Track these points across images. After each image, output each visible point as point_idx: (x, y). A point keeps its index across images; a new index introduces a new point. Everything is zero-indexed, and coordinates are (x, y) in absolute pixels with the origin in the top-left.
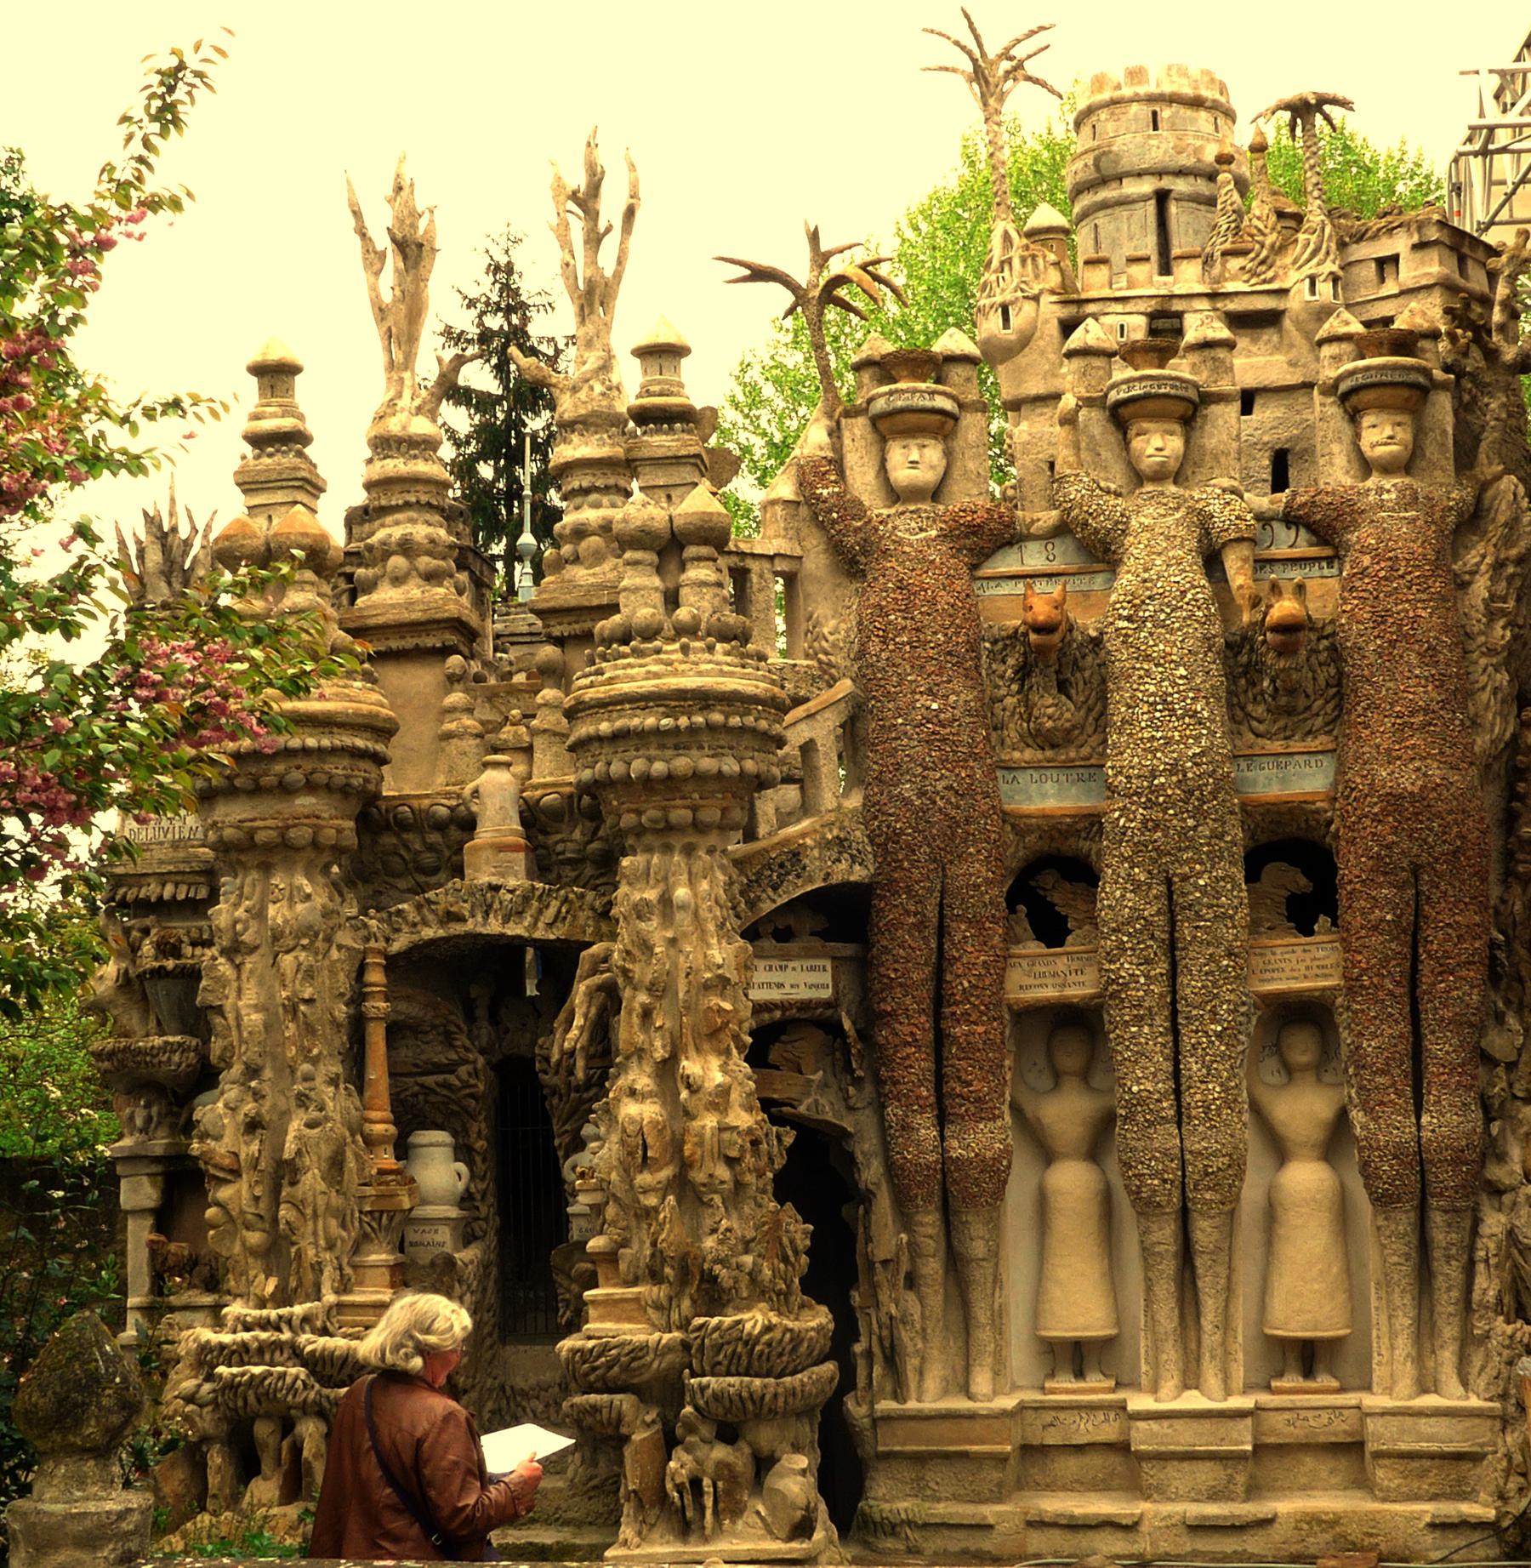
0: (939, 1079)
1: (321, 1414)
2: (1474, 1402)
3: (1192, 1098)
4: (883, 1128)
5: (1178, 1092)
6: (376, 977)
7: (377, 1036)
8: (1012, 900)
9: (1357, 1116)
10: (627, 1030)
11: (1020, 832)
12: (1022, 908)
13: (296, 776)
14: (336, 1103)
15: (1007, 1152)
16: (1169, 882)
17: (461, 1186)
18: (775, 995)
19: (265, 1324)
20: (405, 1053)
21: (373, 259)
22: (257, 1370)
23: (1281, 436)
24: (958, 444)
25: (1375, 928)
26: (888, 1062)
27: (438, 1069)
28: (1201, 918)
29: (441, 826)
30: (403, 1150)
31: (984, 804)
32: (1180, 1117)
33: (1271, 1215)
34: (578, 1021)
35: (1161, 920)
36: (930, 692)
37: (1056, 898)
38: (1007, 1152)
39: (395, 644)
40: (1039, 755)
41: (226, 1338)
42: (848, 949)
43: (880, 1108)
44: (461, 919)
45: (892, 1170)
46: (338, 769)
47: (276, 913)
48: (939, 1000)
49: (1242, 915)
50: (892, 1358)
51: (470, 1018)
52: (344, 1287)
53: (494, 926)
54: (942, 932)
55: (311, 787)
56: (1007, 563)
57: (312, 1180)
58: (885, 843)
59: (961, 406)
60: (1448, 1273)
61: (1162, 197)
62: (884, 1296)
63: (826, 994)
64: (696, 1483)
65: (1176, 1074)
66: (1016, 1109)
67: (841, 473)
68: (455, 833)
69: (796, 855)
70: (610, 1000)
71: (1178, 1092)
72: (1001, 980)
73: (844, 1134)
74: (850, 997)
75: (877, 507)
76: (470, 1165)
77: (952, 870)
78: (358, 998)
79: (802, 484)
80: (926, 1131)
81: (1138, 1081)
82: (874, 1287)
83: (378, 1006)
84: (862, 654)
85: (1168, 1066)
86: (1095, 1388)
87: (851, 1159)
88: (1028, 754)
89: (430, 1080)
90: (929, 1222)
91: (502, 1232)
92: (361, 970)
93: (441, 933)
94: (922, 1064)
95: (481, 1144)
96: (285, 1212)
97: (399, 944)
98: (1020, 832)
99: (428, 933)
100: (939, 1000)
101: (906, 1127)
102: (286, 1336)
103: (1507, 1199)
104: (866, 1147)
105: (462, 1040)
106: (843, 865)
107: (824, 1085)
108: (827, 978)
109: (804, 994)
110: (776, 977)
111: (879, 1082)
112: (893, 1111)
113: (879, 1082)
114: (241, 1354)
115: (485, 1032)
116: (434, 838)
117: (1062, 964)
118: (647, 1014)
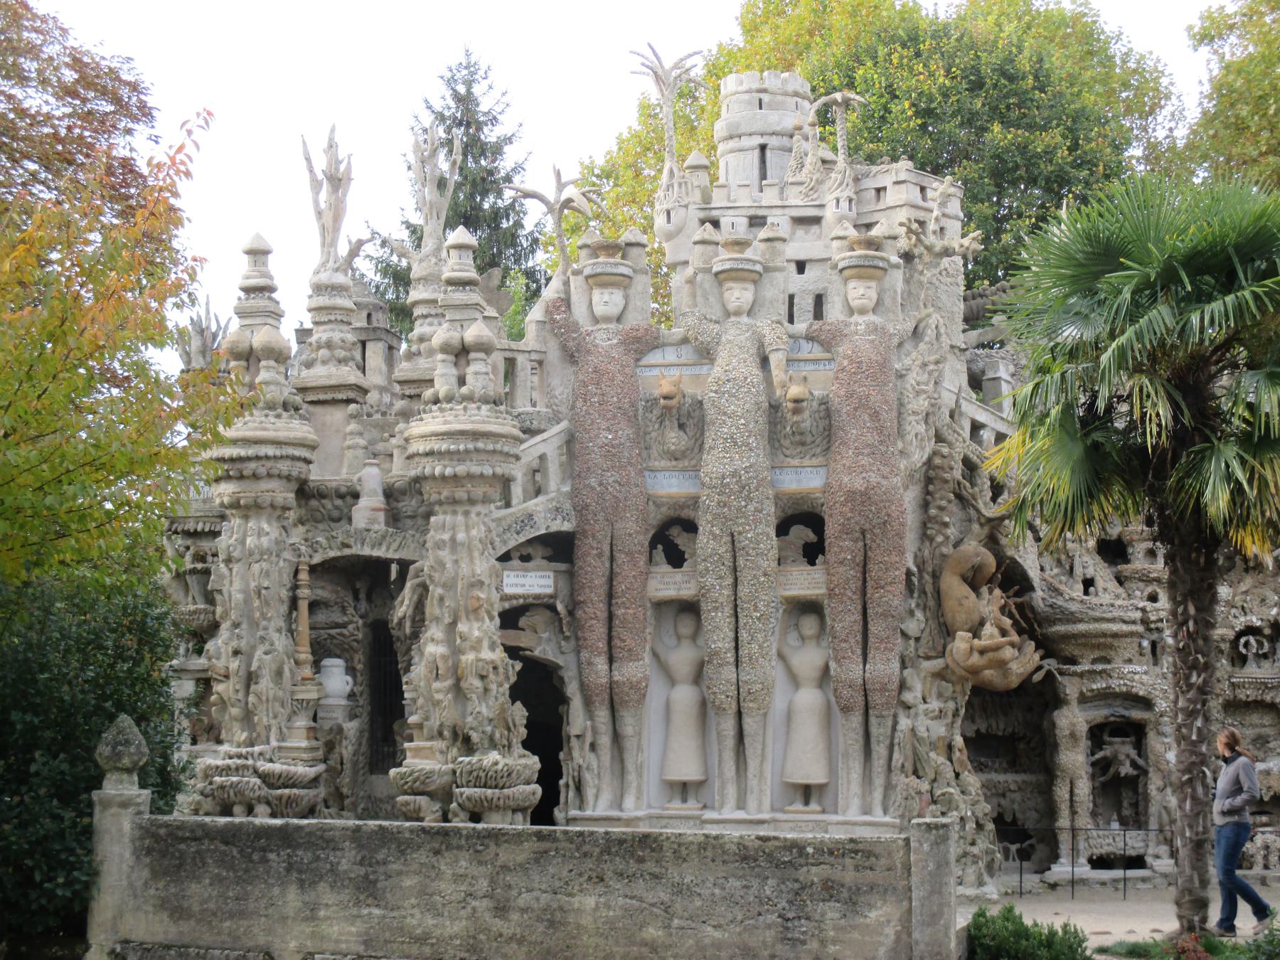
2: (887, 819)
4: (579, 664)
5: (737, 648)
6: (304, 576)
9: (833, 665)
10: (431, 609)
11: (658, 505)
12: (660, 547)
13: (262, 471)
14: (281, 642)
15: (646, 678)
16: (732, 535)
17: (348, 688)
18: (519, 591)
19: (240, 756)
20: (322, 617)
22: (235, 779)
23: (817, 287)
24: (632, 292)
25: (841, 563)
26: (581, 628)
27: (337, 626)
28: (748, 554)
29: (342, 497)
30: (317, 666)
31: (635, 491)
32: (737, 663)
33: (789, 716)
34: (406, 602)
35: (728, 555)
36: (608, 429)
37: (678, 541)
38: (646, 678)
39: (322, 397)
40: (669, 464)
41: (220, 762)
42: (563, 566)
43: (578, 652)
44: (348, 546)
45: (583, 687)
46: (284, 467)
48: (610, 596)
49: (774, 553)
50: (579, 788)
51: (356, 598)
52: (282, 738)
53: (367, 551)
54: (612, 558)
55: (269, 476)
56: (654, 358)
57: (265, 684)
58: (581, 510)
59: (635, 271)
60: (880, 750)
62: (576, 754)
63: (550, 591)
65: (736, 639)
66: (655, 655)
67: (569, 306)
68: (349, 499)
69: (530, 516)
71: (737, 648)
72: (645, 585)
73: (558, 667)
74: (564, 592)
75: (586, 326)
76: (354, 677)
77: (617, 526)
78: (295, 587)
79: (547, 312)
80: (601, 664)
81: (714, 642)
82: (570, 749)
83: (304, 592)
84: (573, 407)
85: (732, 635)
86: (691, 807)
87: (561, 679)
88: (663, 463)
89: (333, 632)
90: (603, 715)
91: (372, 715)
92: (296, 572)
93: (339, 554)
94: (600, 630)
95: (360, 667)
96: (251, 699)
97: (317, 559)
98: (658, 505)
99: (332, 554)
100: (610, 596)
101: (590, 664)
102: (250, 762)
103: (912, 711)
105: (351, 611)
106: (558, 521)
107: (549, 640)
108: (551, 582)
109: (537, 590)
110: (521, 581)
112: (585, 655)
113: (577, 639)
114: (226, 770)
115: (363, 606)
116: (339, 502)
118: (441, 599)
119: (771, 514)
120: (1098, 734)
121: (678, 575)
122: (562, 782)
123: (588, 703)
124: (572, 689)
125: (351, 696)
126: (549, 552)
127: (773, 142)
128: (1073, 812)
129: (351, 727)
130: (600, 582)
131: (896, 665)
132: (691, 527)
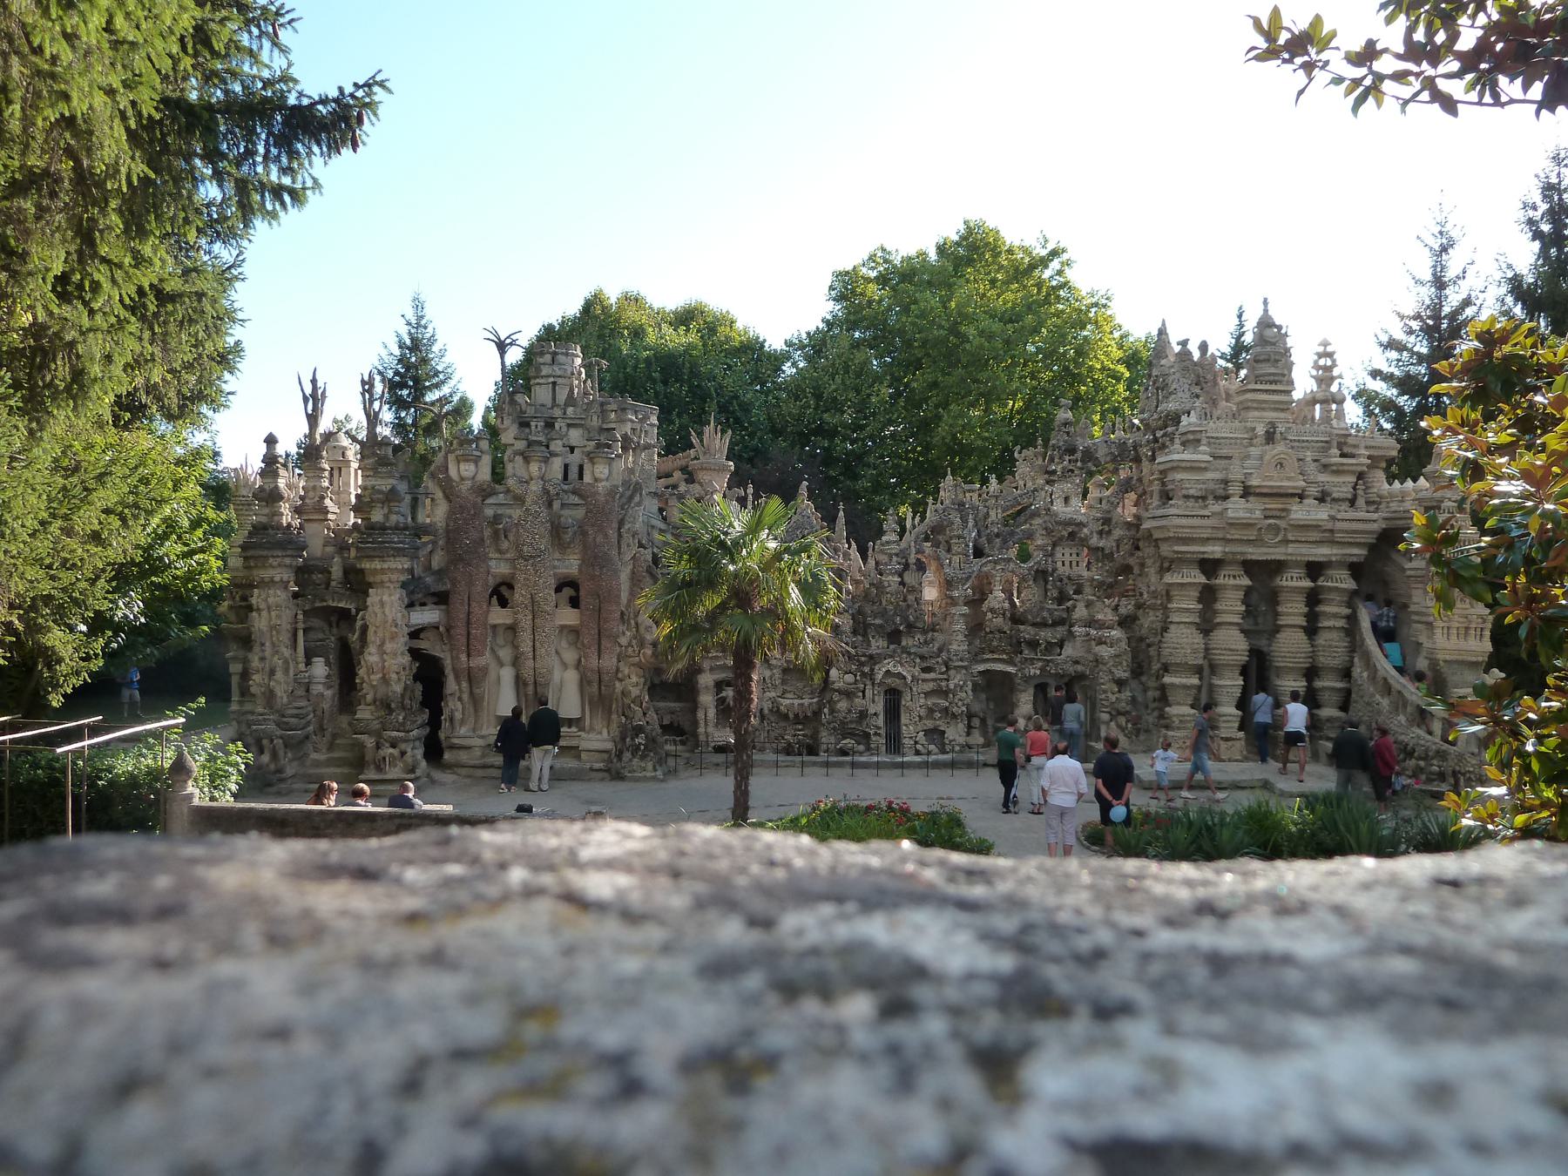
0: (468, 645)
1: (281, 737)
3: (538, 653)
7: (300, 633)
8: (491, 596)
11: (494, 577)
18: (420, 621)
20: (312, 635)
21: (306, 400)
32: (534, 658)
42: (443, 607)
45: (454, 669)
47: (270, 600)
48: (468, 623)
51: (331, 626)
61: (554, 384)
64: (384, 758)
66: (492, 649)
70: (365, 629)
72: (486, 617)
73: (440, 659)
80: (463, 657)
90: (465, 685)
91: (341, 685)
94: (464, 640)
100: (468, 623)
104: (448, 663)
119: (553, 582)
120: (719, 686)
123: (457, 678)
124: (448, 670)
125: (328, 677)
127: (559, 381)
128: (706, 725)
129: (328, 693)
130: (463, 616)
131: (615, 660)
132: (511, 587)
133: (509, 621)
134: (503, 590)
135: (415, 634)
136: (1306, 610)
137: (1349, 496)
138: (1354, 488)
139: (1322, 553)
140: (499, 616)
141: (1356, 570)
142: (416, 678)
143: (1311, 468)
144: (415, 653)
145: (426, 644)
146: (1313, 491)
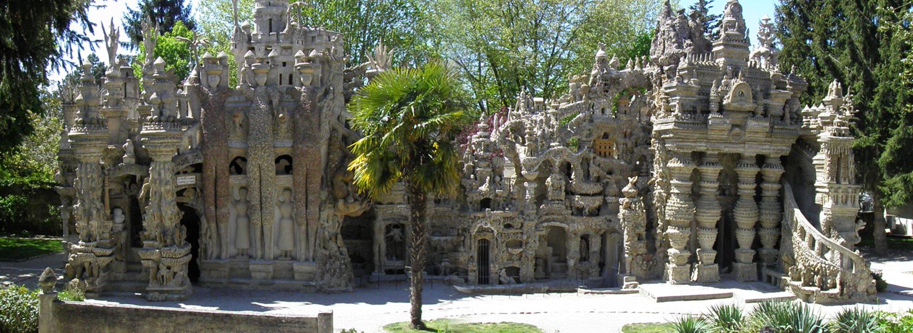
3: (263, 206)
5: (261, 204)
8: (230, 166)
42: (198, 175)
48: (216, 186)
62: (204, 240)
63: (194, 183)
65: (261, 201)
80: (212, 208)
90: (213, 225)
95: (127, 212)
101: (208, 208)
108: (194, 180)
111: (204, 200)
112: (207, 205)
117: (240, 178)
121: (240, 177)
122: (199, 250)
123: (208, 222)
125: (124, 222)
126: (193, 169)
133: (244, 183)
134: (239, 161)
135: (180, 193)
136: (755, 186)
137: (781, 115)
138: (784, 109)
139: (765, 150)
140: (236, 181)
141: (784, 160)
142: (182, 222)
143: (760, 96)
144: (181, 206)
145: (189, 199)
146: (760, 110)
